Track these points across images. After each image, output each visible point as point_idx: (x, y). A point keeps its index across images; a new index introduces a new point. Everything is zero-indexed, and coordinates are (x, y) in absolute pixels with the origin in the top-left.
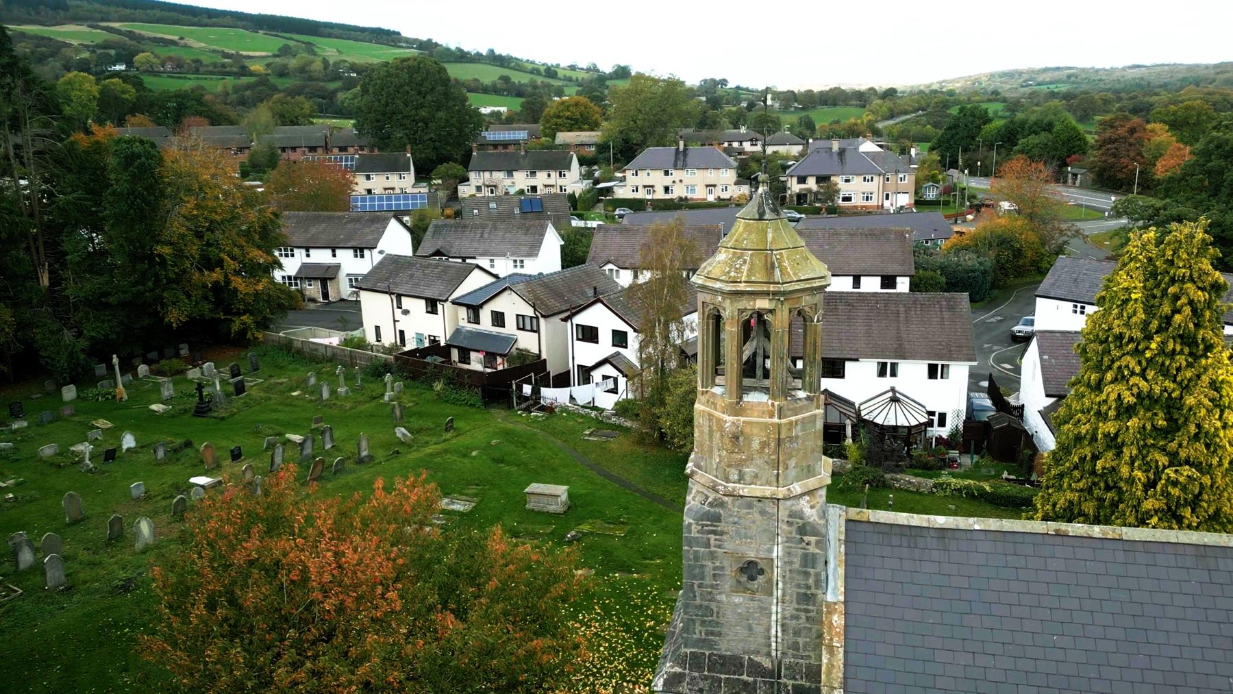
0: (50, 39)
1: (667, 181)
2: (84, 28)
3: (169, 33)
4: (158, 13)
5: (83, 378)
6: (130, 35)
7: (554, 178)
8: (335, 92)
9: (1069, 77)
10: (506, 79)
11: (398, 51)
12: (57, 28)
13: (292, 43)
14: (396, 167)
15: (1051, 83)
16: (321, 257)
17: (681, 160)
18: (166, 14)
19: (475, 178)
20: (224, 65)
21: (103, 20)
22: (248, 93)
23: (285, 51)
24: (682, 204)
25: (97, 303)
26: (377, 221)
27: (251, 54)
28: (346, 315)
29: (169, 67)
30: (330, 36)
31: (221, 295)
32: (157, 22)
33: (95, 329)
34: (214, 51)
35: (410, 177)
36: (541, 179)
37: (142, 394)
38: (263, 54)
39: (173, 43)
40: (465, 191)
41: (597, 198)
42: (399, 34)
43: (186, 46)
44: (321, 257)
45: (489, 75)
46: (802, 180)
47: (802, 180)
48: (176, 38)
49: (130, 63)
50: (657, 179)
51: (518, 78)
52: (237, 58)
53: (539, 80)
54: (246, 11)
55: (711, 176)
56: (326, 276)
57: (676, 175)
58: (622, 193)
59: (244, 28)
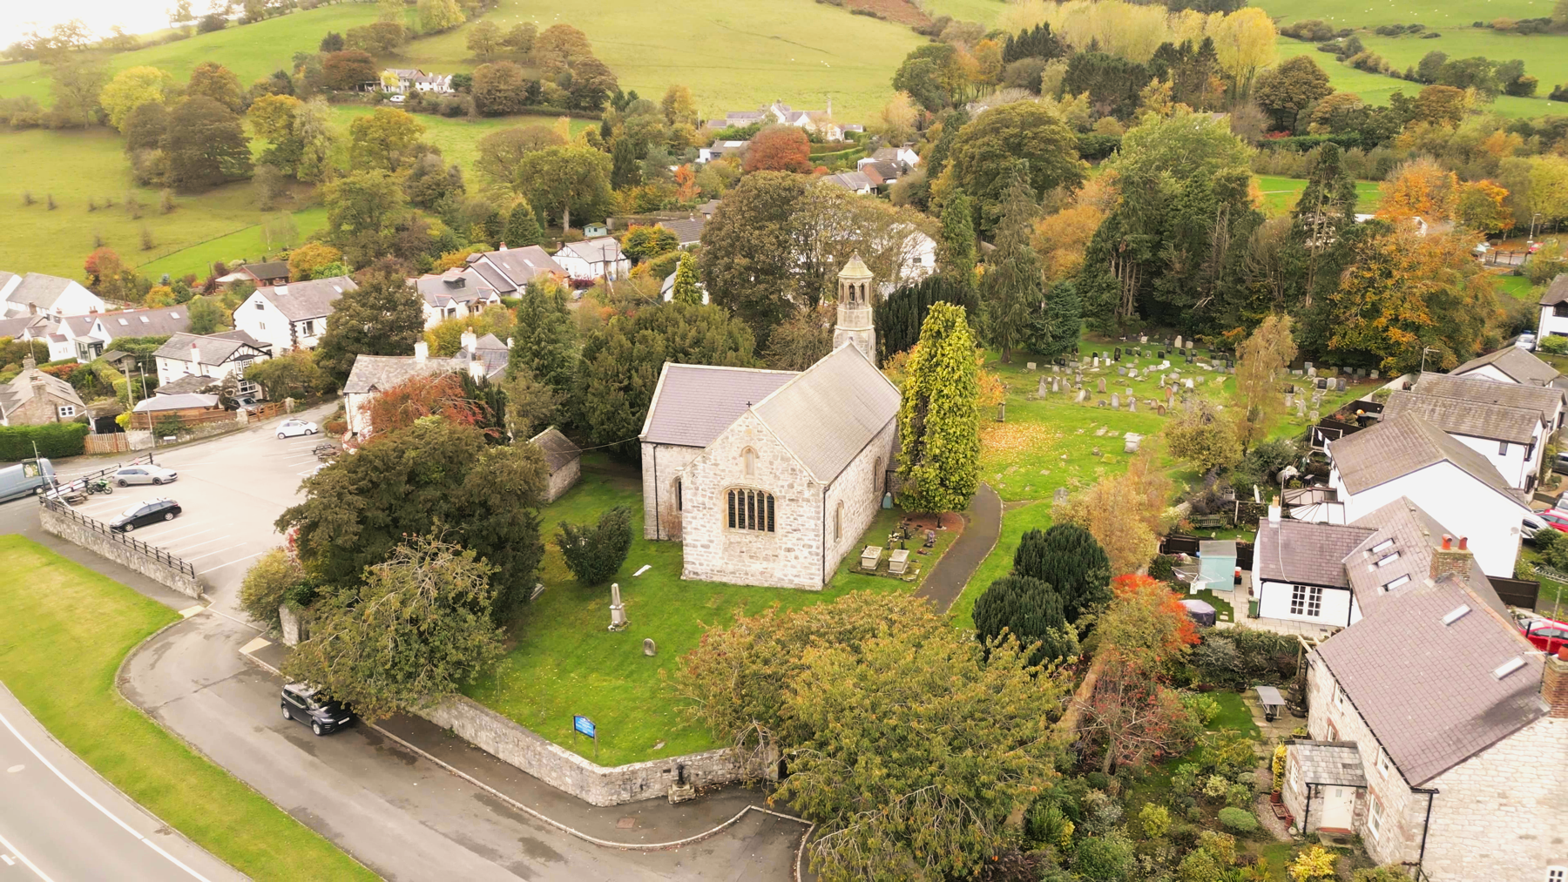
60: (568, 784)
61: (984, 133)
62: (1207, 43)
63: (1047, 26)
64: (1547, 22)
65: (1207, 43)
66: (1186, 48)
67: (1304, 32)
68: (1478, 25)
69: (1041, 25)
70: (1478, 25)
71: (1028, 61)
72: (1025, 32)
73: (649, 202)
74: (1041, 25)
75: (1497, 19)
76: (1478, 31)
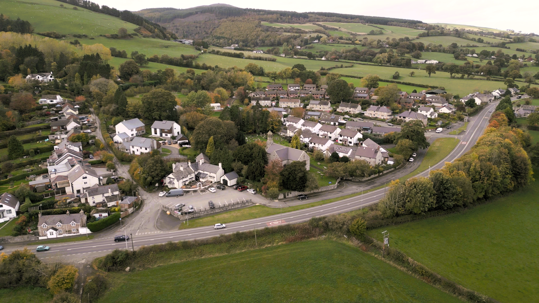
0: (300, 30)
1: (374, 113)
4: (335, 18)
5: (259, 134)
6: (324, 27)
7: (354, 110)
10: (455, 46)
11: (418, 31)
14: (326, 104)
18: (338, 18)
19: (340, 108)
20: (350, 40)
21: (317, 21)
22: (348, 53)
23: (372, 33)
25: (261, 127)
27: (360, 34)
32: (334, 21)
33: (261, 129)
36: (352, 109)
37: (263, 136)
38: (364, 33)
39: (337, 29)
41: (361, 115)
42: (421, 22)
43: (340, 31)
46: (400, 117)
47: (400, 117)
48: (337, 28)
49: (319, 40)
50: (373, 113)
51: (461, 43)
52: (355, 35)
53: (472, 43)
55: (383, 113)
57: (376, 112)
59: (362, 23)
60: (332, 188)
61: (159, 97)
62: (98, 55)
63: (30, 45)
64: (117, 35)
65: (98, 55)
66: (93, 55)
67: (52, 35)
68: (101, 35)
69: (28, 45)
70: (101, 35)
71: (32, 58)
72: (21, 47)
73: (5, 126)
74: (28, 45)
75: (106, 34)
76: (101, 38)
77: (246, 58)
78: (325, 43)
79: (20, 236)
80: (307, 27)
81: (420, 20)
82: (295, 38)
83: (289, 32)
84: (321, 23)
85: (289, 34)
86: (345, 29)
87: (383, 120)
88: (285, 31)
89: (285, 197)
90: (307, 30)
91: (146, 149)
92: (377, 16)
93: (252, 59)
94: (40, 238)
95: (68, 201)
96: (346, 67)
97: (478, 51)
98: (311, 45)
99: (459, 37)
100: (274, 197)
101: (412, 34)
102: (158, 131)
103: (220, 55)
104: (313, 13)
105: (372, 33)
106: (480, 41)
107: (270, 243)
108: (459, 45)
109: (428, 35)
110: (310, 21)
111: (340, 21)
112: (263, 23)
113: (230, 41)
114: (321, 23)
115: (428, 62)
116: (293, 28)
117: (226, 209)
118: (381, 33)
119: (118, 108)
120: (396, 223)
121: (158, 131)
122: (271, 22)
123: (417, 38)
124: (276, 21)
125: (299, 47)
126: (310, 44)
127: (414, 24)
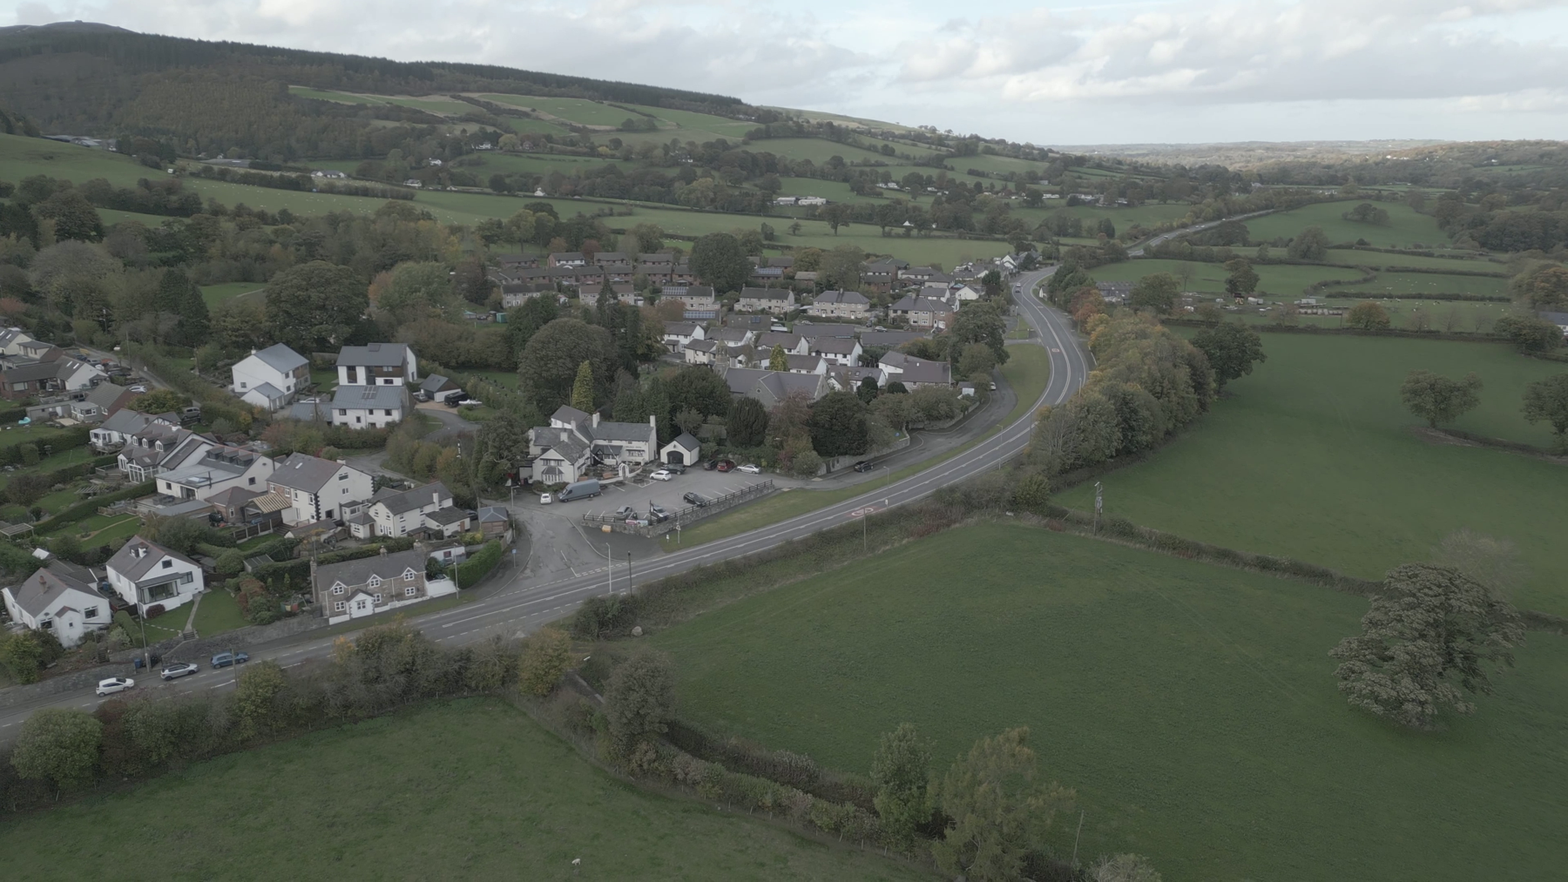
2: (446, 99)
3: (521, 103)
6: (487, 105)
7: (779, 303)
8: (673, 180)
9: (1542, 156)
10: (837, 162)
11: (736, 124)
12: (424, 99)
13: (634, 117)
15: (1518, 163)
16: (673, 337)
17: (840, 300)
19: (743, 301)
20: (573, 144)
21: (464, 90)
23: (628, 127)
24: (838, 320)
26: (694, 322)
27: (597, 127)
28: (682, 356)
29: (527, 145)
30: (670, 107)
31: (649, 347)
34: (563, 124)
35: (710, 300)
36: (774, 303)
39: (526, 115)
40: (737, 307)
41: (800, 314)
42: (738, 102)
43: (537, 118)
44: (673, 337)
45: (820, 153)
48: (527, 109)
50: (828, 306)
51: (852, 156)
52: (584, 131)
53: (874, 158)
54: (592, 77)
56: (675, 344)
58: (811, 313)
59: (590, 98)
77: (321, 191)
78: (514, 152)
79: (278, 623)
80: (436, 104)
81: (737, 96)
82: (420, 135)
83: (387, 118)
84: (475, 95)
85: (390, 124)
86: (549, 113)
87: (859, 322)
88: (378, 117)
89: (829, 471)
90: (441, 115)
91: (388, 413)
92: (649, 84)
93: (340, 193)
94: (333, 621)
95: (324, 537)
96: (620, 214)
97: (900, 173)
98: (474, 156)
99: (838, 141)
100: (810, 472)
101: (732, 132)
102: (361, 373)
103: (233, 181)
104: (443, 65)
105: (628, 127)
106: (887, 151)
107: (886, 543)
108: (847, 161)
109: (767, 135)
110: (440, 89)
111: (529, 93)
112: (293, 89)
113: (191, 143)
114: (475, 95)
115: (803, 202)
116: (399, 108)
117: (729, 505)
118: (652, 129)
119: (181, 324)
120: (1070, 485)
121: (361, 373)
122: (320, 87)
123: (745, 143)
124: (336, 85)
125: (438, 162)
126: (468, 153)
127: (726, 107)
